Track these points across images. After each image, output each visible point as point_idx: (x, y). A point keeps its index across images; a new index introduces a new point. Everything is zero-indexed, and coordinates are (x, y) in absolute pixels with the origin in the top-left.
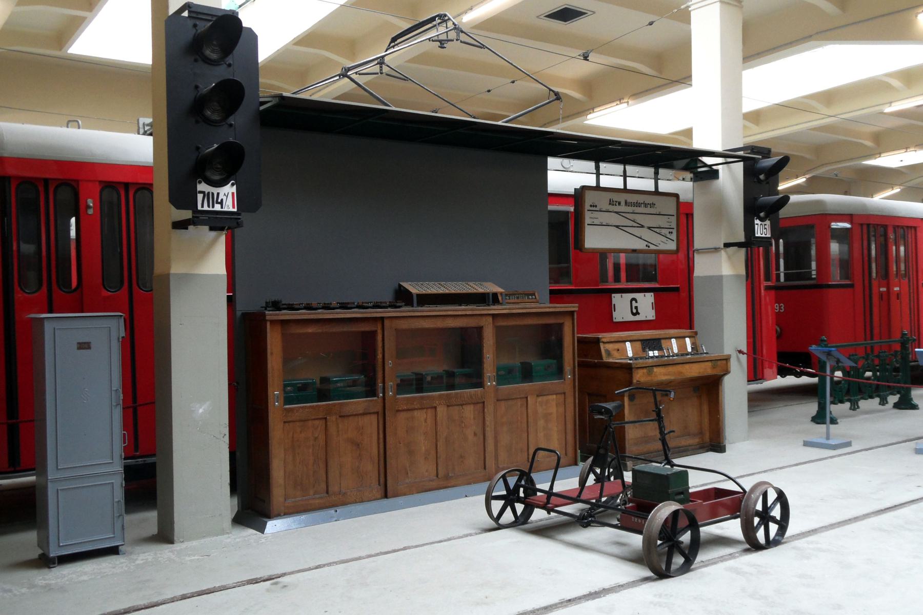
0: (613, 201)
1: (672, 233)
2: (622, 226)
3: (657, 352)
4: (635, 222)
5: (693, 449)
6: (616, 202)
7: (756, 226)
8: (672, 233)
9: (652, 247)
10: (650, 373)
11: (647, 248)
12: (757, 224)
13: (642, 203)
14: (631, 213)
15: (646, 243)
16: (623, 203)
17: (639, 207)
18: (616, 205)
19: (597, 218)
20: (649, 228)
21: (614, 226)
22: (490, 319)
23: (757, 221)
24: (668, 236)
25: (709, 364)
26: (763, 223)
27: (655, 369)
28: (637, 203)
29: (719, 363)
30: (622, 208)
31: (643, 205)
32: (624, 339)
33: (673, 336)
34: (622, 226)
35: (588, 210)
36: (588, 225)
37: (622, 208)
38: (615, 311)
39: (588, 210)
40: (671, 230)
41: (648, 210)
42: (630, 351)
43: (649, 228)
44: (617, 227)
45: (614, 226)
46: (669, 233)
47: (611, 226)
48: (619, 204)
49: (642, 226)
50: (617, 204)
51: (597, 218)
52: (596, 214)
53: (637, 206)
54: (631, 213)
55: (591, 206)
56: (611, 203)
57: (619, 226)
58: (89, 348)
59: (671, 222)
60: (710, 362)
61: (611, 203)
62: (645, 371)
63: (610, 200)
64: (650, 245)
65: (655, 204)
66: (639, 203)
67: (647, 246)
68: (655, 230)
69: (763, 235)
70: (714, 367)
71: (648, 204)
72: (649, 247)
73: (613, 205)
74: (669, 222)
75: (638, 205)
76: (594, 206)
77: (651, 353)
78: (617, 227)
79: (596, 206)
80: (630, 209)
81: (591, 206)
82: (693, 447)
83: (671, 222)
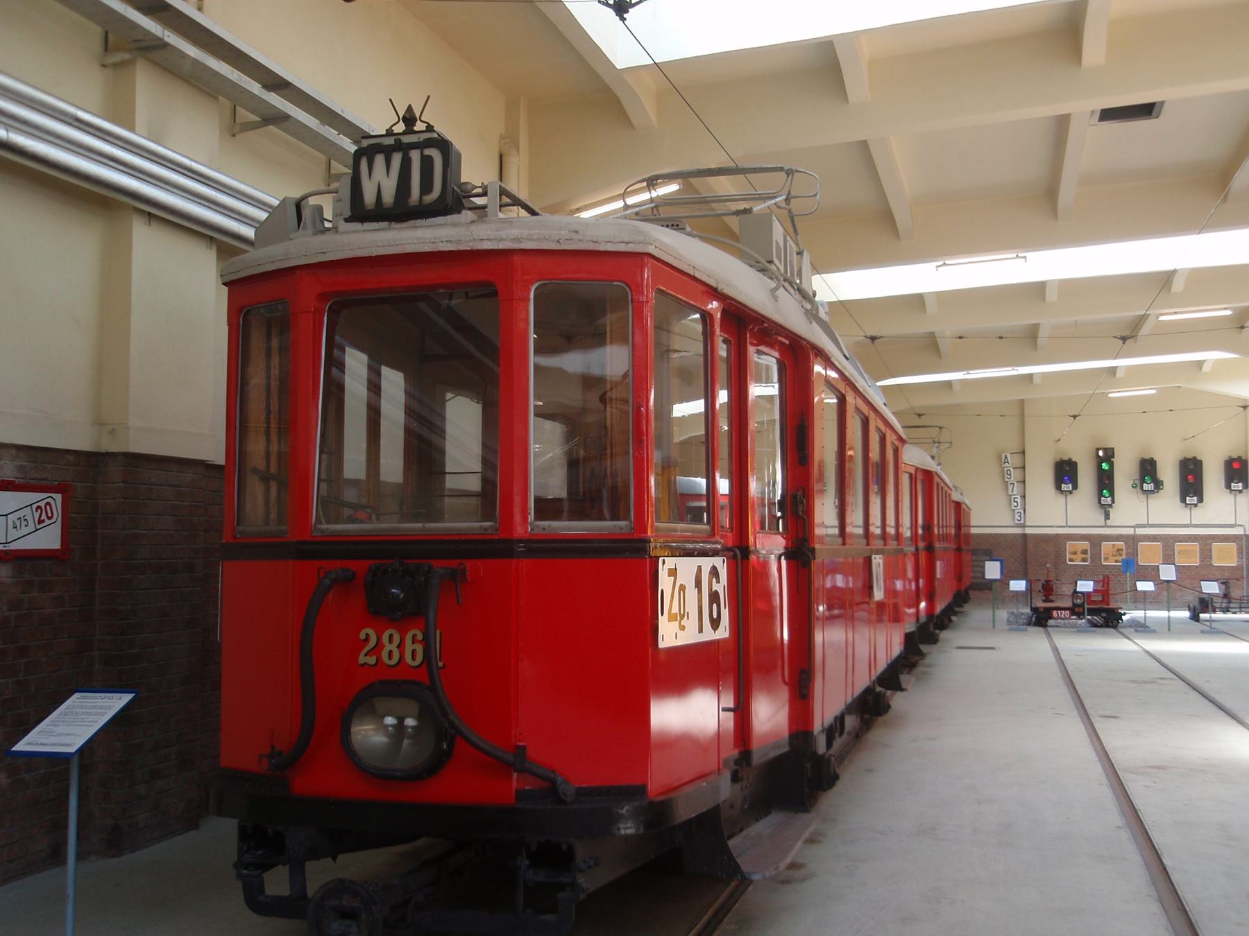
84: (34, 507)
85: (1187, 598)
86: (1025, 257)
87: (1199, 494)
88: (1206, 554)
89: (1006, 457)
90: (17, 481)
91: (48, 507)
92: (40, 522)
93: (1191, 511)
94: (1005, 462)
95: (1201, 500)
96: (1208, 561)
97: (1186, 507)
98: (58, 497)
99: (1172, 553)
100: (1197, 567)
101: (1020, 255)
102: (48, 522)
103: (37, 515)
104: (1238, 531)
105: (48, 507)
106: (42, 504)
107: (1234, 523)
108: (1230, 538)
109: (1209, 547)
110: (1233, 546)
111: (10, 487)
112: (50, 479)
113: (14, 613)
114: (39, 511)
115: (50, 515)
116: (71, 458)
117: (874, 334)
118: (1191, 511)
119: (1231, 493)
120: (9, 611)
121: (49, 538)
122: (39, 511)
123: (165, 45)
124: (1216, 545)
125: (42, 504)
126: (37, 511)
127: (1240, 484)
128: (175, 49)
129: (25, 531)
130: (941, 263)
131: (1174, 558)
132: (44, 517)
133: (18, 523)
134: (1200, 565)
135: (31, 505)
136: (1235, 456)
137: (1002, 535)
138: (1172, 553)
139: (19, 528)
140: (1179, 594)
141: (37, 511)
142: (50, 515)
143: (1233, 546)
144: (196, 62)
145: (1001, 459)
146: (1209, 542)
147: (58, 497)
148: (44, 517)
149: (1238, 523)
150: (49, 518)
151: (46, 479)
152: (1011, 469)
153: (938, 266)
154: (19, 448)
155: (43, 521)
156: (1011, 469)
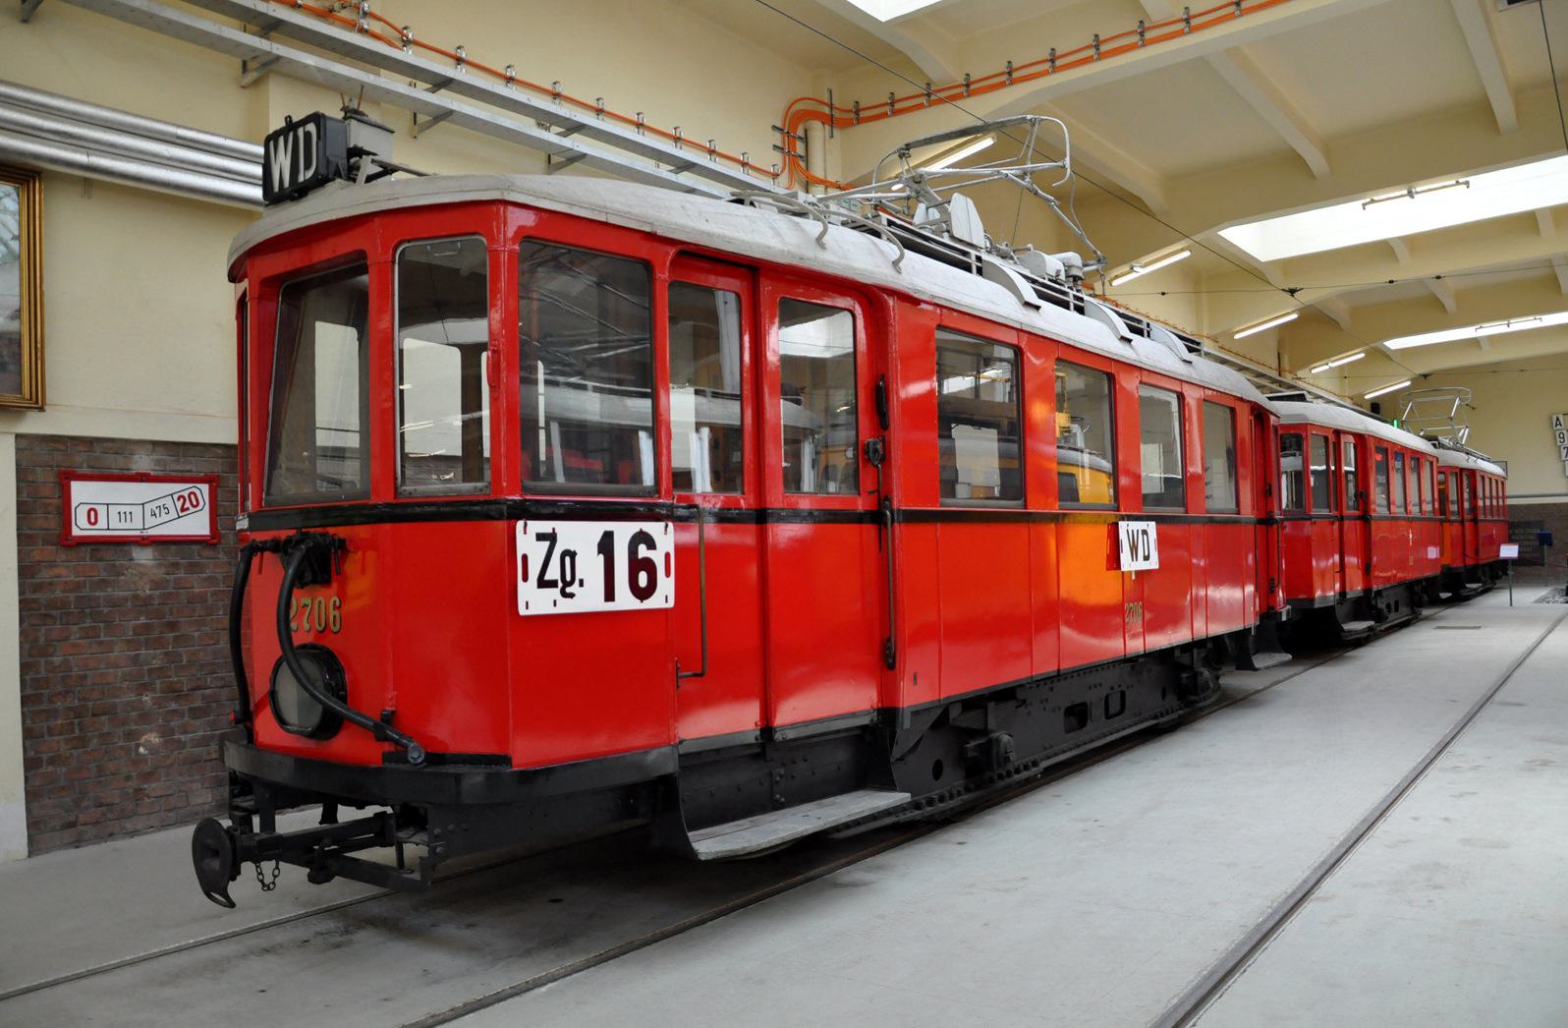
84: (176, 497)
86: (1467, 183)
89: (1558, 419)
90: (152, 473)
91: (192, 497)
92: (183, 510)
94: (1557, 425)
98: (205, 488)
101: (1461, 180)
102: (192, 510)
103: (179, 504)
105: (192, 497)
106: (185, 494)
111: (144, 478)
112: (194, 470)
113: (158, 592)
114: (182, 500)
115: (195, 503)
116: (220, 451)
117: (1292, 286)
120: (150, 590)
121: (197, 524)
122: (182, 500)
123: (278, 58)
125: (185, 494)
126: (179, 499)
128: (290, 61)
129: (165, 518)
130: (1368, 200)
132: (188, 505)
133: (157, 512)
135: (172, 495)
137: (1555, 504)
139: (158, 515)
141: (179, 499)
142: (195, 503)
144: (320, 70)
145: (1552, 422)
147: (205, 488)
148: (188, 505)
150: (194, 506)
151: (190, 471)
152: (1565, 432)
153: (1364, 205)
154: (155, 443)
155: (188, 509)
156: (1565, 432)
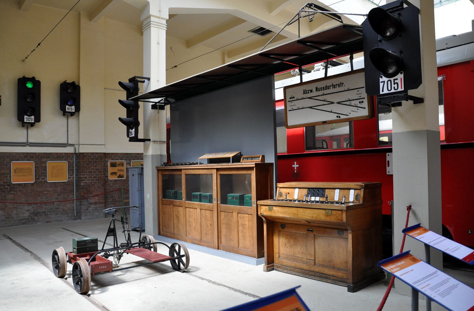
0: (306, 91)
1: (362, 102)
2: (314, 106)
3: (319, 198)
4: (326, 101)
5: (333, 280)
6: (309, 90)
7: (381, 85)
8: (362, 102)
9: (342, 117)
10: (270, 210)
11: (338, 118)
12: (384, 82)
13: (331, 86)
14: (321, 95)
15: (337, 115)
16: (314, 90)
17: (328, 89)
18: (308, 93)
19: (295, 105)
20: (339, 103)
21: (308, 107)
22: (215, 170)
23: (384, 79)
24: (359, 105)
25: (323, 212)
26: (392, 79)
27: (274, 208)
28: (326, 87)
29: (334, 212)
30: (315, 93)
31: (331, 87)
32: (294, 187)
33: (338, 187)
34: (314, 106)
35: (289, 102)
36: (289, 111)
37: (315, 93)
38: (388, 166)
39: (289, 102)
40: (361, 100)
41: (338, 89)
42: (296, 195)
43: (339, 103)
44: (311, 108)
45: (308, 107)
46: (360, 102)
47: (306, 108)
48: (311, 91)
49: (332, 103)
50: (310, 92)
51: (295, 105)
52: (294, 103)
53: (326, 89)
54: (321, 95)
55: (290, 98)
56: (305, 92)
57: (313, 107)
58: (134, 174)
59: (361, 94)
60: (324, 210)
61: (305, 92)
62: (267, 207)
63: (304, 90)
64: (340, 115)
65: (343, 83)
66: (328, 86)
67: (337, 117)
68: (348, 103)
69: (393, 91)
70: (327, 215)
71: (337, 85)
72: (340, 117)
73: (306, 93)
74: (358, 94)
75: (327, 88)
76: (292, 98)
77: (313, 199)
78: (311, 108)
79: (294, 98)
80: (320, 93)
81: (290, 98)
82: (335, 278)
83: (361, 94)
85: (22, 215)
87: (36, 112)
88: (41, 171)
93: (27, 131)
95: (38, 119)
96: (43, 179)
97: (23, 126)
99: (8, 171)
100: (33, 184)
104: (69, 150)
107: (66, 142)
108: (63, 157)
109: (44, 165)
110: (64, 164)
118: (27, 131)
119: (64, 115)
124: (50, 164)
127: (73, 107)
131: (10, 176)
134: (36, 182)
136: (69, 81)
138: (8, 171)
140: (15, 212)
143: (64, 164)
146: (43, 160)
149: (70, 142)
